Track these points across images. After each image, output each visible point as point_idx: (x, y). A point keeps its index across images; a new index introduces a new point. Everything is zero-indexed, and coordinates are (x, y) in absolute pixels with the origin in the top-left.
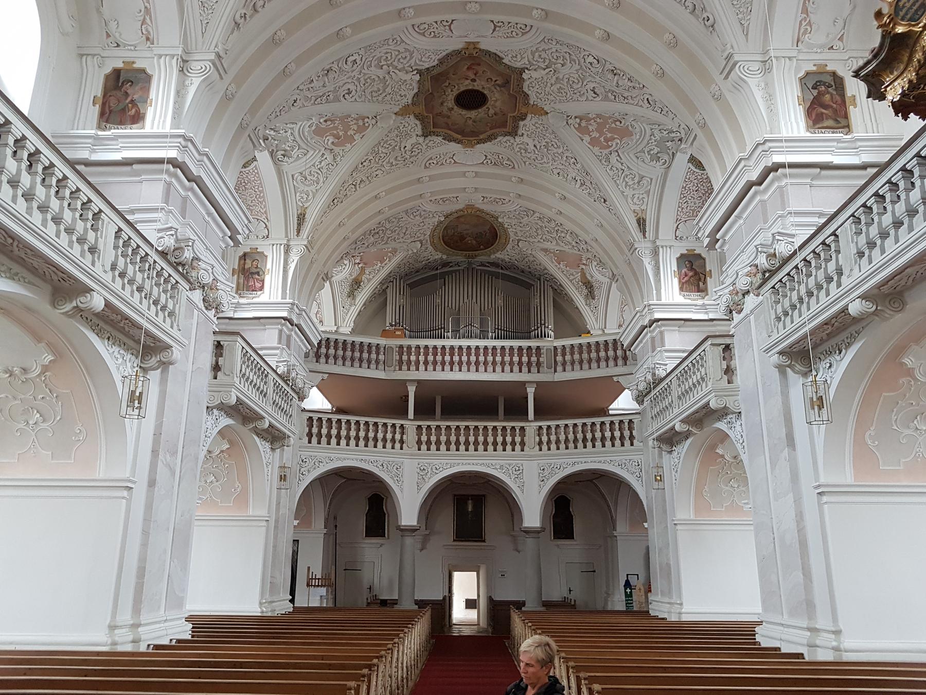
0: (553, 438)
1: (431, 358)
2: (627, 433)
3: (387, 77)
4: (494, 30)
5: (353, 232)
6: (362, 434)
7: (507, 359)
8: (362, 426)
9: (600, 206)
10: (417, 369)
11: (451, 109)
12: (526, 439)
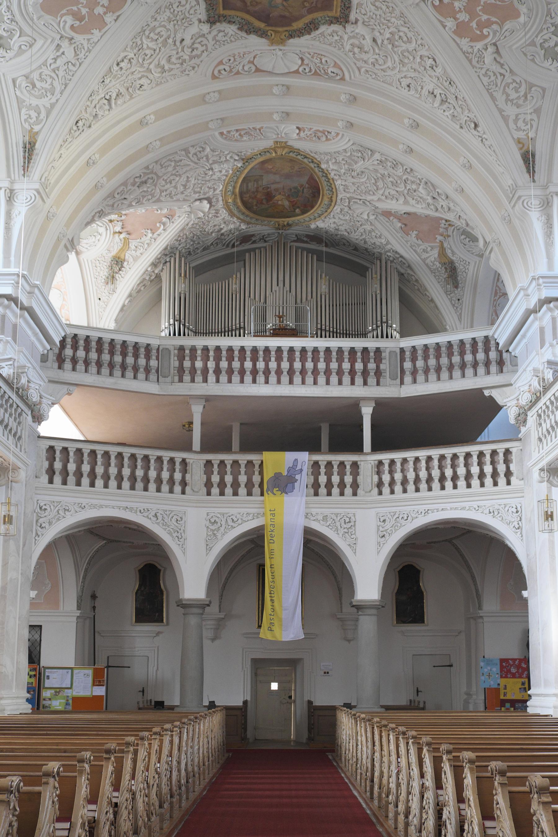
0: (398, 476)
1: (224, 364)
2: (502, 468)
5: (110, 176)
6: (126, 472)
7: (334, 365)
8: (126, 460)
9: (469, 136)
10: (205, 380)
12: (360, 479)
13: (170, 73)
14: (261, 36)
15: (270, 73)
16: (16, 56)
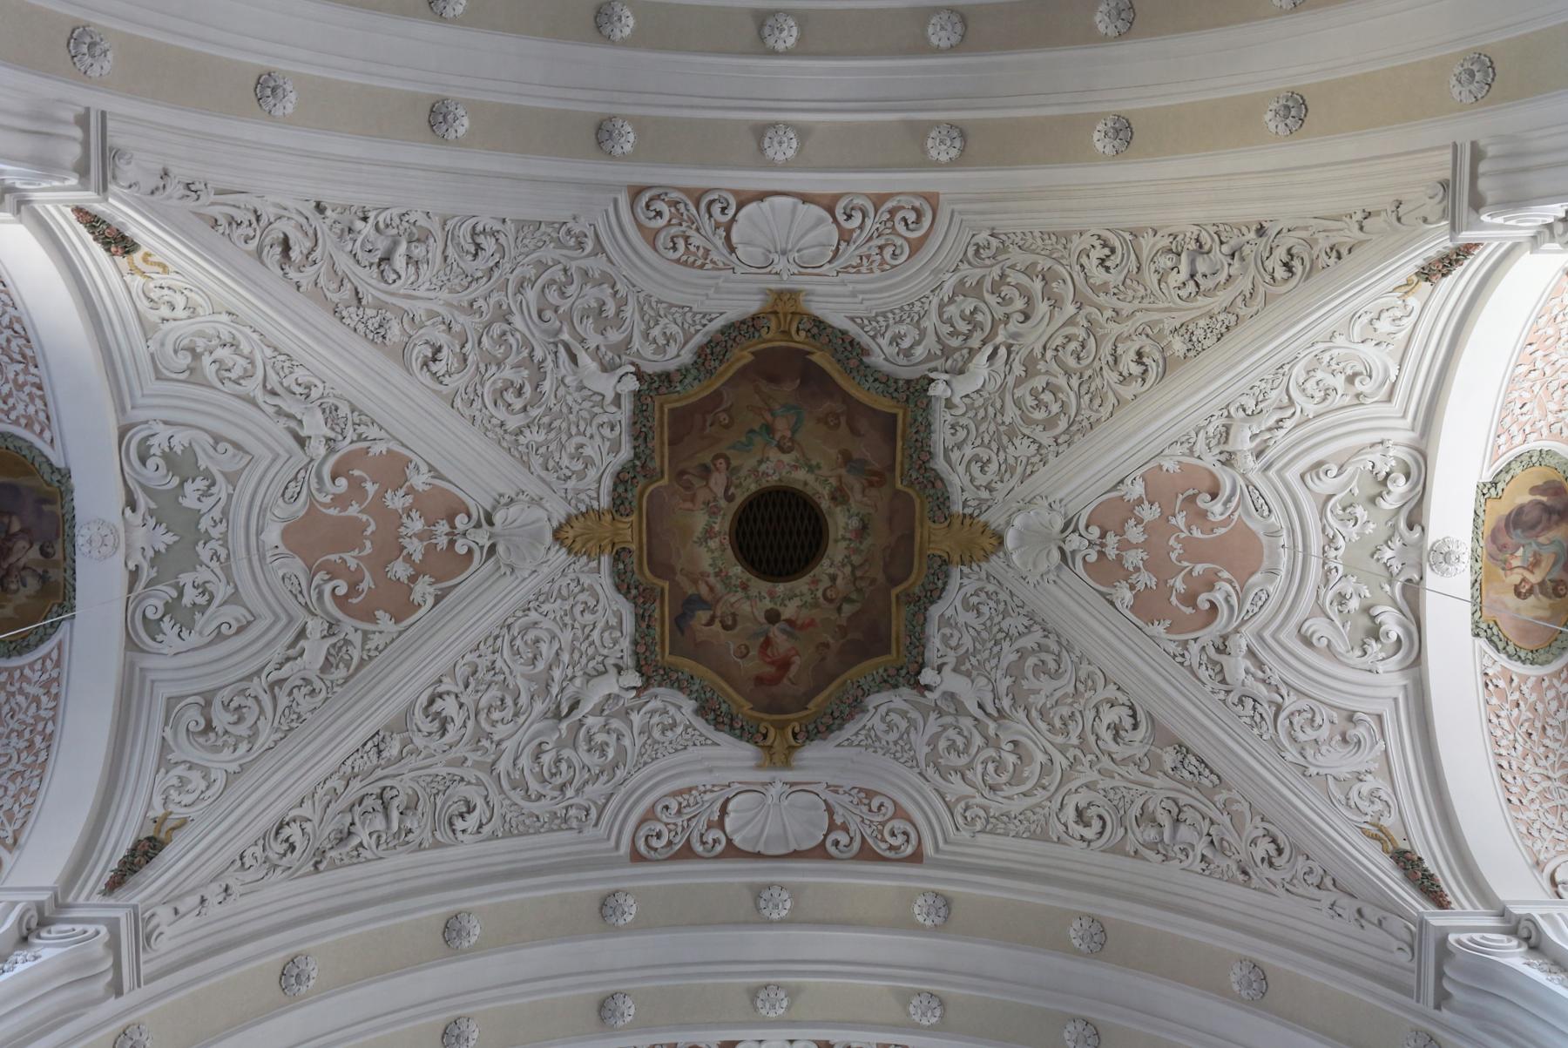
3: (1006, 703)
4: (723, 811)
11: (840, 496)
13: (1030, 258)
14: (818, 323)
15: (806, 199)
16: (1360, 451)
